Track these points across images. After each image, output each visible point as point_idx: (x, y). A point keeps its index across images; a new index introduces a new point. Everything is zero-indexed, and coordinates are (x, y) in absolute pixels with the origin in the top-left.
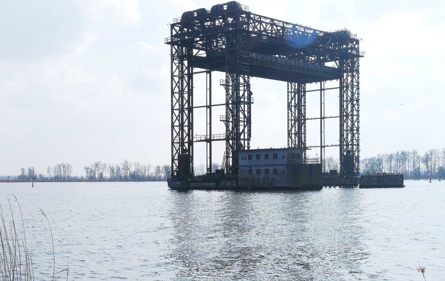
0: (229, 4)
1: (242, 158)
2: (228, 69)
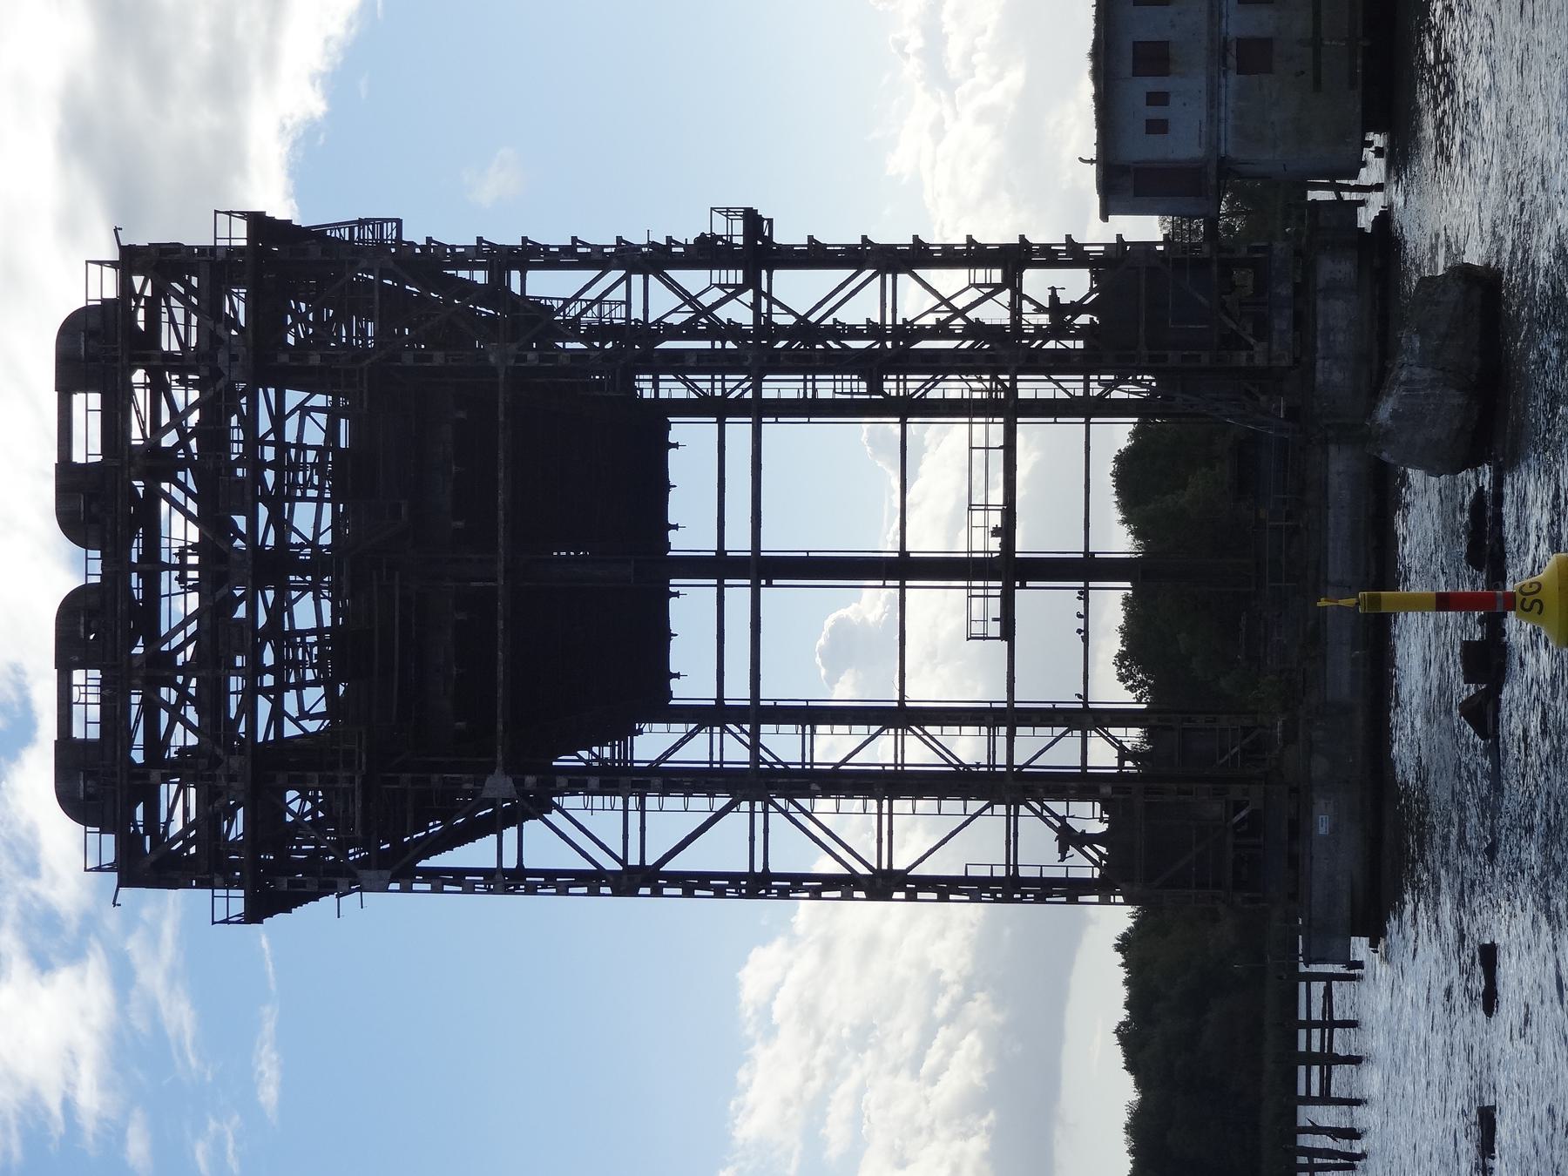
0: (71, 378)
1: (1157, 127)
2: (513, 348)
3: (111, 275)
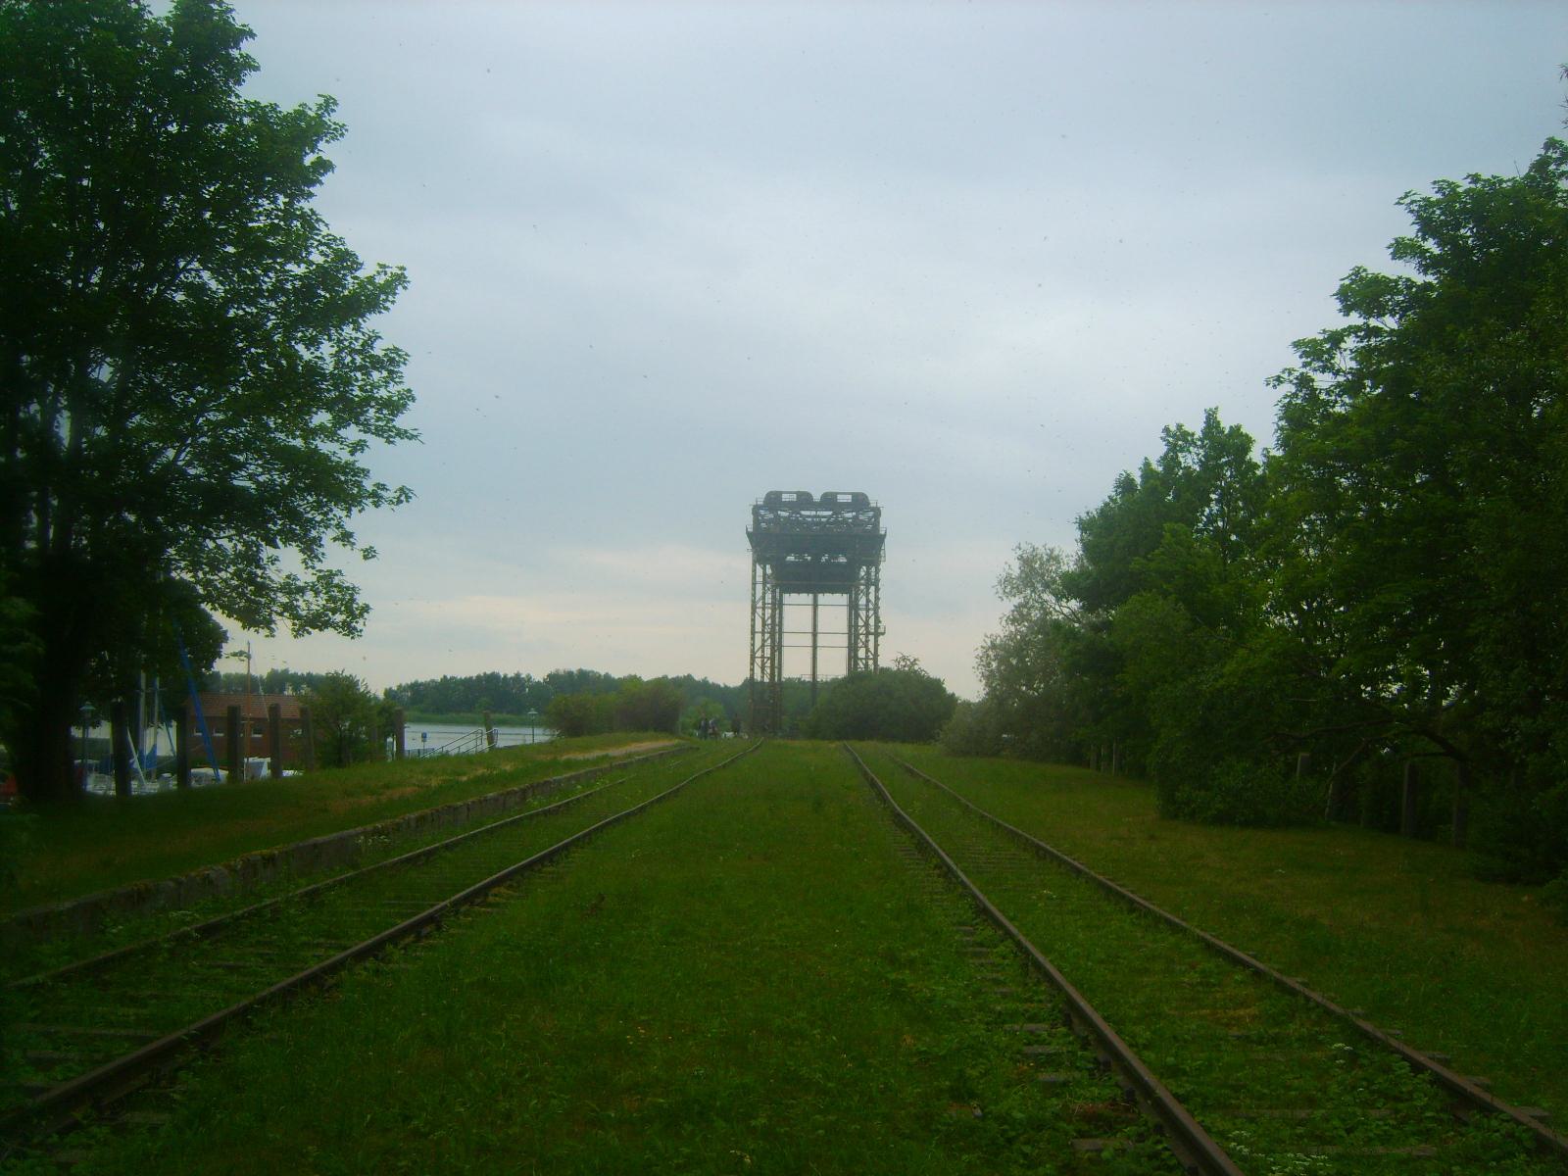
0: (855, 496)
3: (875, 505)
